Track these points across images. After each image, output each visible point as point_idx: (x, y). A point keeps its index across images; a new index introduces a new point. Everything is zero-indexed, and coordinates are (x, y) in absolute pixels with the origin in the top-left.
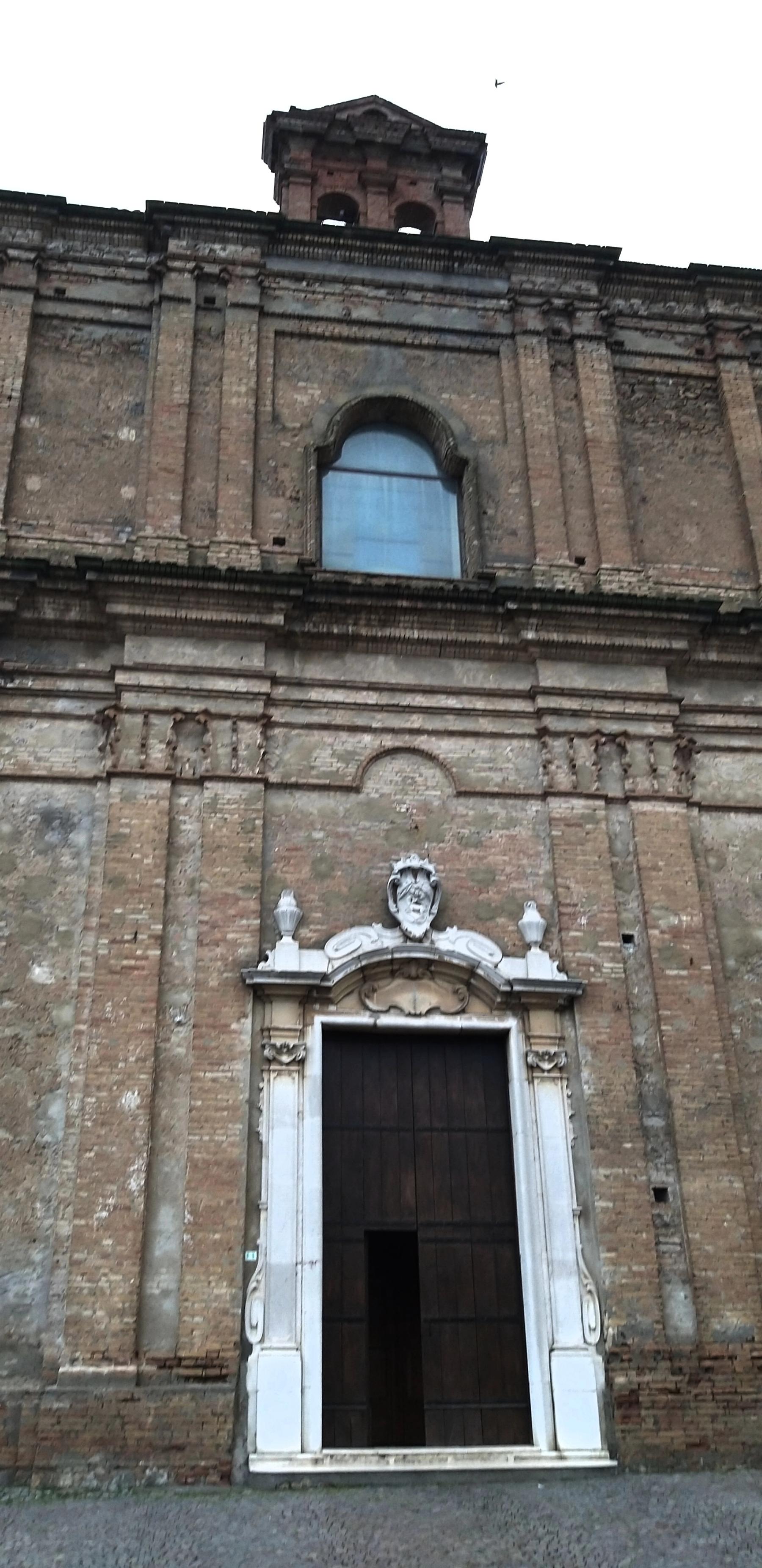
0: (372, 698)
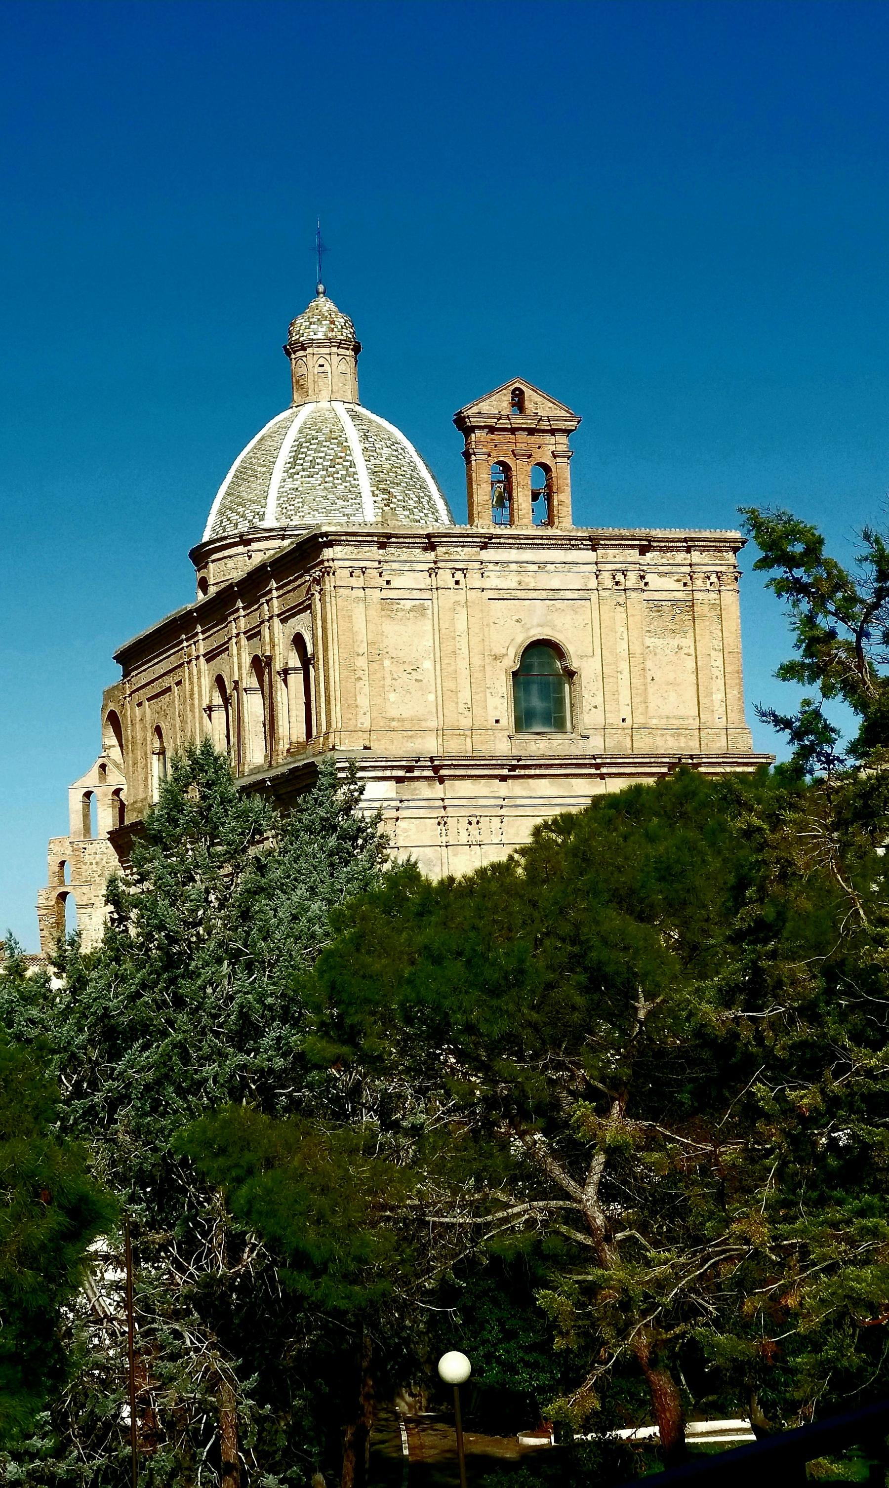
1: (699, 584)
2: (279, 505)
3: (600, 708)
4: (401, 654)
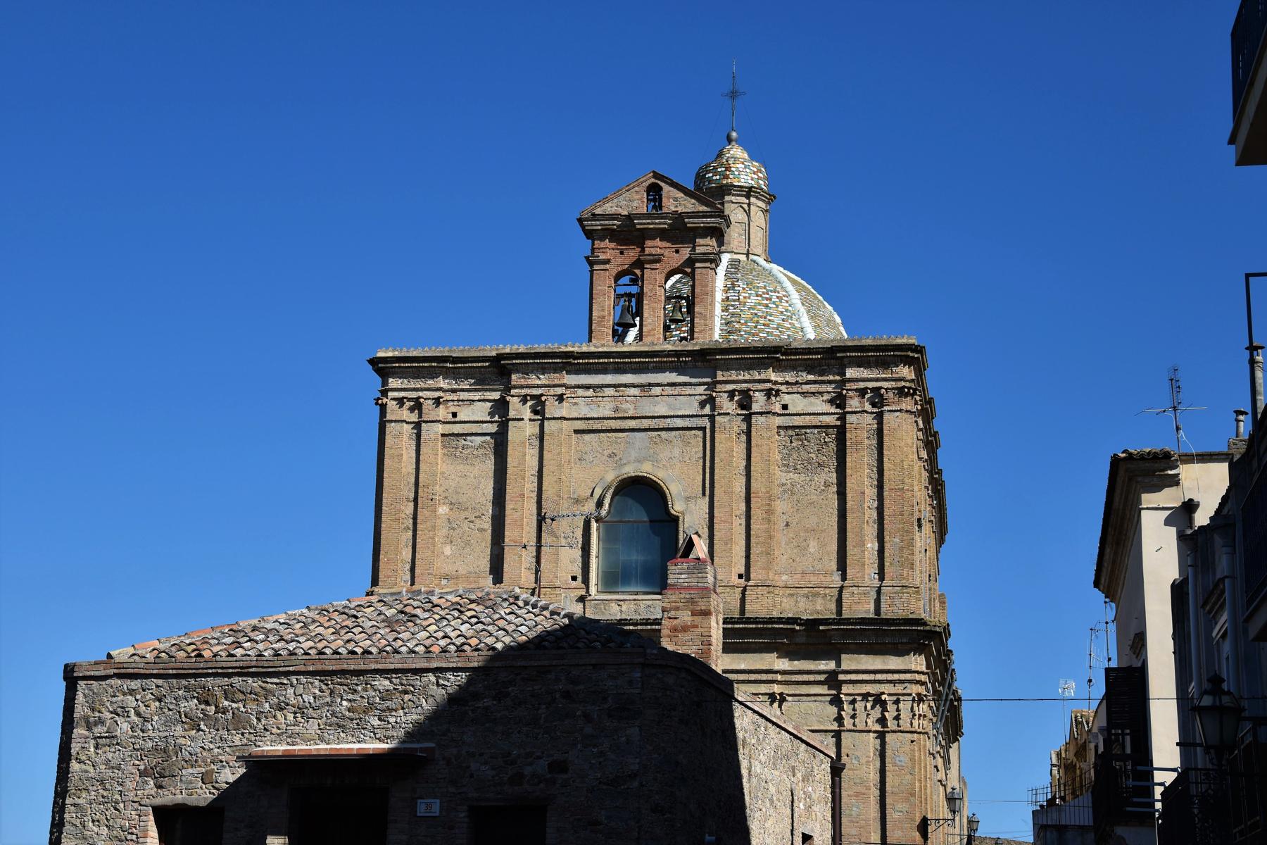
1: (854, 403)
4: (463, 499)
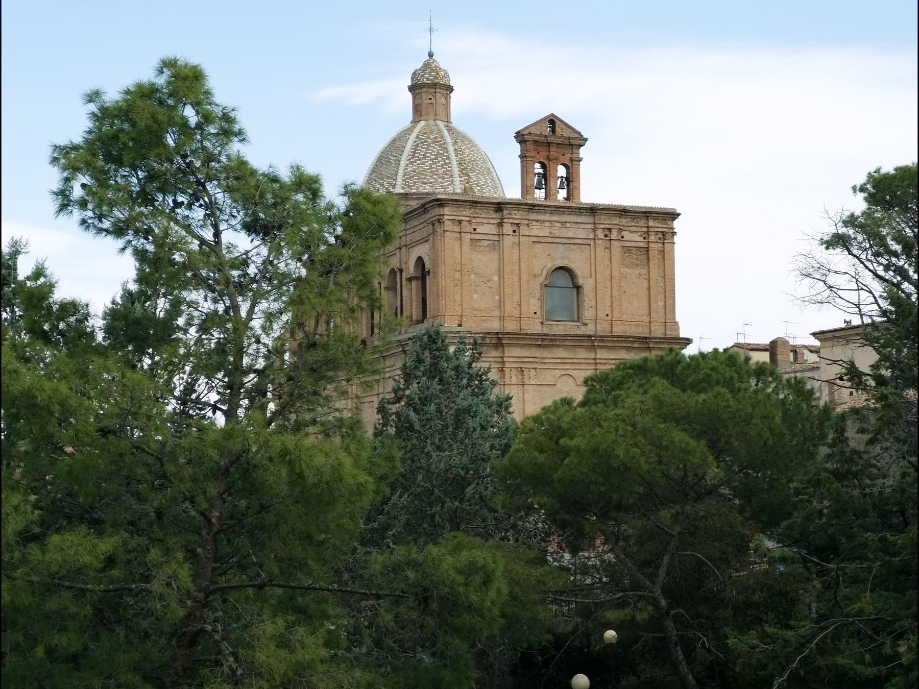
0: (559, 361)
1: (652, 238)
2: (404, 180)
3: (594, 308)
